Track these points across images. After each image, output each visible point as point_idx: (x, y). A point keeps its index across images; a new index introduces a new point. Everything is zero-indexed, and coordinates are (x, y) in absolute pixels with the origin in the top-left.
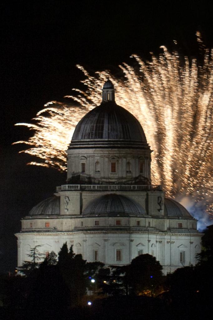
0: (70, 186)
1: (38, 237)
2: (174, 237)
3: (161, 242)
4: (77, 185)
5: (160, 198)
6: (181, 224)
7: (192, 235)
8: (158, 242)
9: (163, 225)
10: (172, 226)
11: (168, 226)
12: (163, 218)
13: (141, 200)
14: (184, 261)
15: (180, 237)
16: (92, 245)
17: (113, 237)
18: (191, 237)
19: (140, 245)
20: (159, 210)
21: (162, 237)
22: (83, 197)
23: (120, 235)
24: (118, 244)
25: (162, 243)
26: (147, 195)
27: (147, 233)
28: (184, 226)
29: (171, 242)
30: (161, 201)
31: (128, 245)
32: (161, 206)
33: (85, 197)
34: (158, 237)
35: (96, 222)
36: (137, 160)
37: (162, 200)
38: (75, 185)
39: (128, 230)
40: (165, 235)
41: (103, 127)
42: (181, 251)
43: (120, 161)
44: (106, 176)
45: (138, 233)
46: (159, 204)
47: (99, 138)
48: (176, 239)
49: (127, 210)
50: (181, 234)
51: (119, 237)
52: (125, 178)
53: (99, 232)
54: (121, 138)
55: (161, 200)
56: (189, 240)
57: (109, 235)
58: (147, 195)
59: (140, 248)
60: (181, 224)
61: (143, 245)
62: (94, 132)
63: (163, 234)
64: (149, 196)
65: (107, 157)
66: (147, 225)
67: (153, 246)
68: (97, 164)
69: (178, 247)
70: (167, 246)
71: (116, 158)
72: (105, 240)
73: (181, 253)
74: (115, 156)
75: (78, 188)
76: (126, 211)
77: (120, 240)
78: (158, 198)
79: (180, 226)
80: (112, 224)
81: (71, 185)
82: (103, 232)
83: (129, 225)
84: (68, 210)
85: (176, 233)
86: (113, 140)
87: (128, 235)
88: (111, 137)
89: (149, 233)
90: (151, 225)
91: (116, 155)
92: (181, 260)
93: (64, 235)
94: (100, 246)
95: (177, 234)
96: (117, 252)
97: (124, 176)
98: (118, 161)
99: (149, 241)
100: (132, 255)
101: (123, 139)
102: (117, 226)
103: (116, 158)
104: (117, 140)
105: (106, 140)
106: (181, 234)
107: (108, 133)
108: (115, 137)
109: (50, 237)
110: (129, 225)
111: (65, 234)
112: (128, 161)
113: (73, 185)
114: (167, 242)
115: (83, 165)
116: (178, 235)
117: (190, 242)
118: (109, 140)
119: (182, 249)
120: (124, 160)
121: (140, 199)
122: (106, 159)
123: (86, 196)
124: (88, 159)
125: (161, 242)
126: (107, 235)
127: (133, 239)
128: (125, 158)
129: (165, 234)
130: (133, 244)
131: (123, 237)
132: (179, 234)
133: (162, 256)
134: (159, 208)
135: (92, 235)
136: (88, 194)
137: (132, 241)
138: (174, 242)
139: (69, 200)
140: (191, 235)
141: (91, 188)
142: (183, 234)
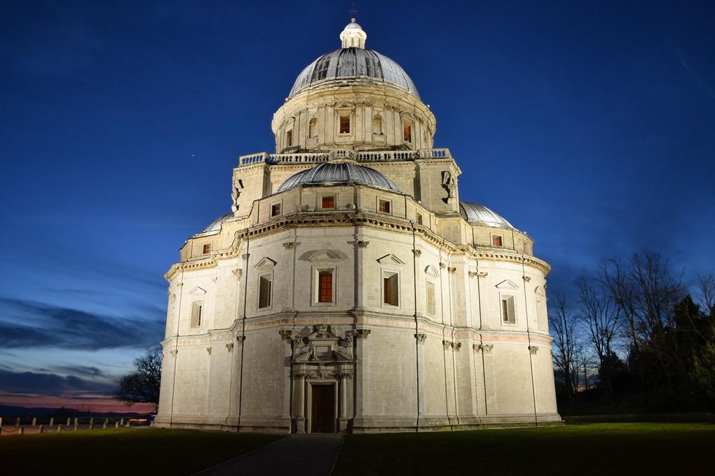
0: (248, 159)
1: (186, 274)
2: (484, 265)
3: (455, 269)
4: (260, 154)
5: (445, 174)
6: (501, 237)
7: (526, 261)
8: (446, 269)
9: (457, 231)
10: (478, 242)
11: (470, 240)
12: (455, 215)
13: (404, 181)
14: (513, 321)
15: (500, 263)
16: (260, 264)
17: (309, 237)
18: (525, 267)
19: (388, 259)
20: (445, 200)
21: (456, 258)
22: (272, 179)
23: (330, 231)
24: (325, 256)
25: (456, 271)
26: (417, 169)
27: (409, 229)
28: (506, 242)
29: (479, 273)
30: (449, 180)
31: (352, 257)
32: (448, 191)
33: (277, 179)
34: (444, 255)
35: (273, 207)
36: (397, 114)
37: (453, 177)
38: (256, 155)
39: (355, 219)
40: (464, 254)
41: (328, 63)
42: (503, 296)
43: (359, 111)
44: (330, 140)
45: (381, 224)
46: (445, 187)
47: (319, 79)
48: (490, 268)
49: (355, 176)
50: (502, 256)
51: (326, 236)
52: (369, 144)
53: (274, 226)
54: (362, 74)
55: (448, 177)
56: (520, 271)
57: (300, 231)
58: (417, 169)
59: (389, 268)
60: (501, 237)
61: (396, 260)
62: (311, 74)
63: (459, 251)
64: (420, 171)
65: (331, 106)
66: (412, 217)
67: (429, 269)
68: (312, 124)
69: (496, 286)
70: (470, 283)
71: (349, 105)
72: (289, 245)
73: (504, 302)
74: (350, 103)
75: (261, 159)
76: (351, 178)
77: (329, 244)
78: (443, 173)
79: (499, 241)
80: (310, 205)
81: (249, 156)
82: (282, 223)
83: (356, 207)
84: (238, 207)
85: (489, 253)
86: (348, 77)
87: (352, 229)
88: (342, 73)
89: (414, 230)
90: (426, 222)
91: (351, 101)
92: (506, 319)
93: (221, 259)
94: (275, 263)
95: (492, 256)
96: (321, 275)
97: (369, 139)
98: (354, 111)
99: (416, 253)
100: (362, 284)
101: (366, 76)
102: (324, 209)
103: (349, 105)
104: (354, 77)
105: (334, 78)
106: (502, 256)
107: (337, 69)
108: (350, 74)
109: (205, 271)
110: (356, 207)
111: (222, 255)
112: (376, 113)
113: (253, 156)
114: (469, 273)
115: (290, 134)
116: (495, 258)
117: (523, 277)
118: (337, 78)
119: (506, 291)
120: (368, 109)
121: (401, 178)
122: (330, 110)
123: (279, 176)
124: (297, 118)
125: (455, 269)
126: (292, 230)
127: (365, 239)
128: (369, 105)
129: (462, 250)
130: (367, 254)
131: (340, 236)
132: (497, 256)
133: (459, 304)
134: (445, 194)
135: (259, 241)
136: (283, 173)
137: (361, 244)
138: (487, 275)
139: (243, 187)
140: (524, 259)
141: (290, 161)
142: (506, 257)
